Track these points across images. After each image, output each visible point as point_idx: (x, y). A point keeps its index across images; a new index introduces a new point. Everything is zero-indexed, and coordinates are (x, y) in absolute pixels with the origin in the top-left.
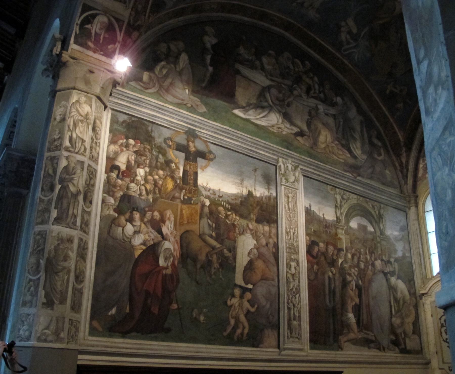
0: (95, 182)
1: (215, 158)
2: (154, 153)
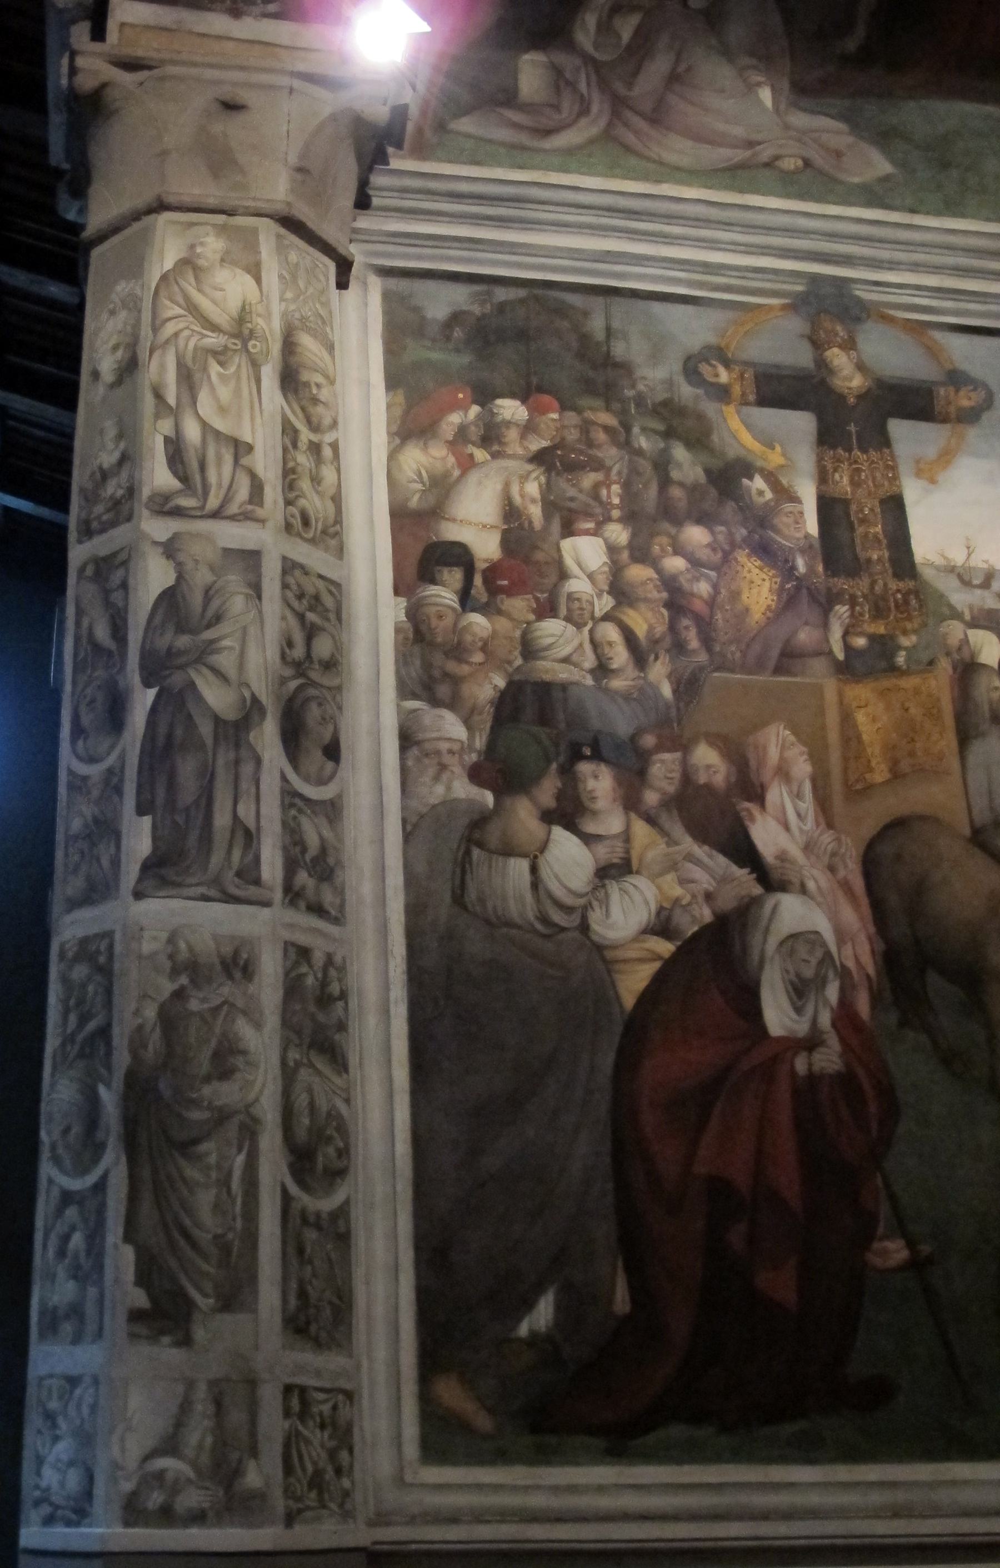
0: (338, 647)
1: (988, 403)
2: (643, 442)
